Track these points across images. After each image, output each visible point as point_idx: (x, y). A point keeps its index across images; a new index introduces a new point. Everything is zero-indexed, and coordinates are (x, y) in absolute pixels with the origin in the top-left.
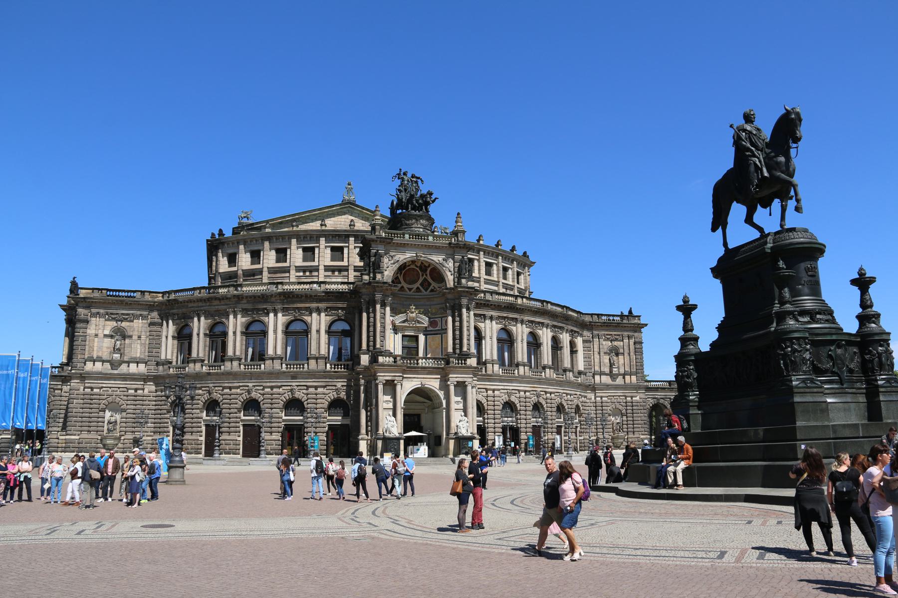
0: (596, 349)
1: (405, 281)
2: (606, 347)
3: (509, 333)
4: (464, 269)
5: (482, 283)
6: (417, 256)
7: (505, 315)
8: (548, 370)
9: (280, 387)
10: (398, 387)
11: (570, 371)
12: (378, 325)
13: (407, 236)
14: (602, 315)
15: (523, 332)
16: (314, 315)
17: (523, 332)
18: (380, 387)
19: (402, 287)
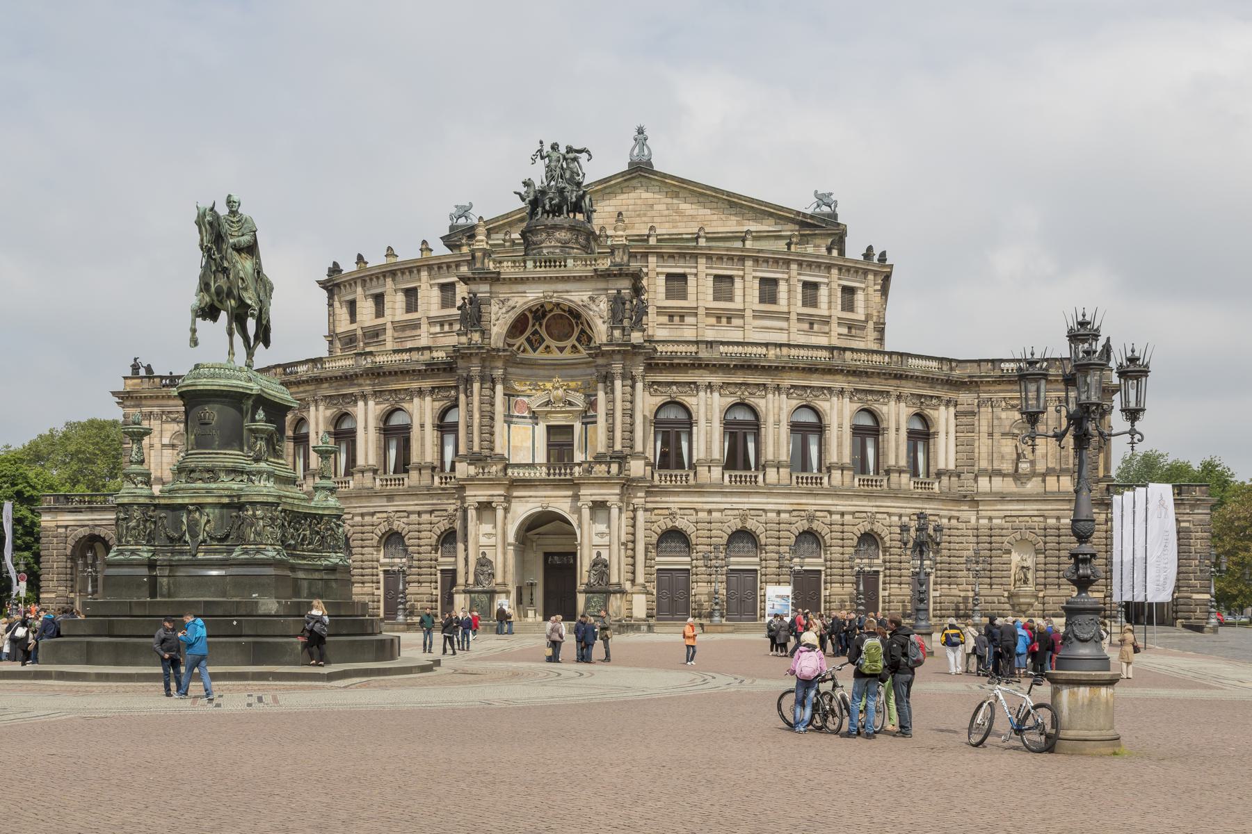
0: (984, 428)
1: (551, 335)
2: (1007, 423)
3: (753, 410)
4: (629, 310)
5: (749, 319)
6: (545, 297)
7: (739, 380)
8: (836, 474)
9: (373, 514)
10: (500, 513)
11: (900, 472)
12: (476, 415)
13: (530, 264)
14: (1002, 361)
15: (780, 409)
16: (416, 400)
17: (780, 409)
18: (472, 513)
19: (548, 347)
